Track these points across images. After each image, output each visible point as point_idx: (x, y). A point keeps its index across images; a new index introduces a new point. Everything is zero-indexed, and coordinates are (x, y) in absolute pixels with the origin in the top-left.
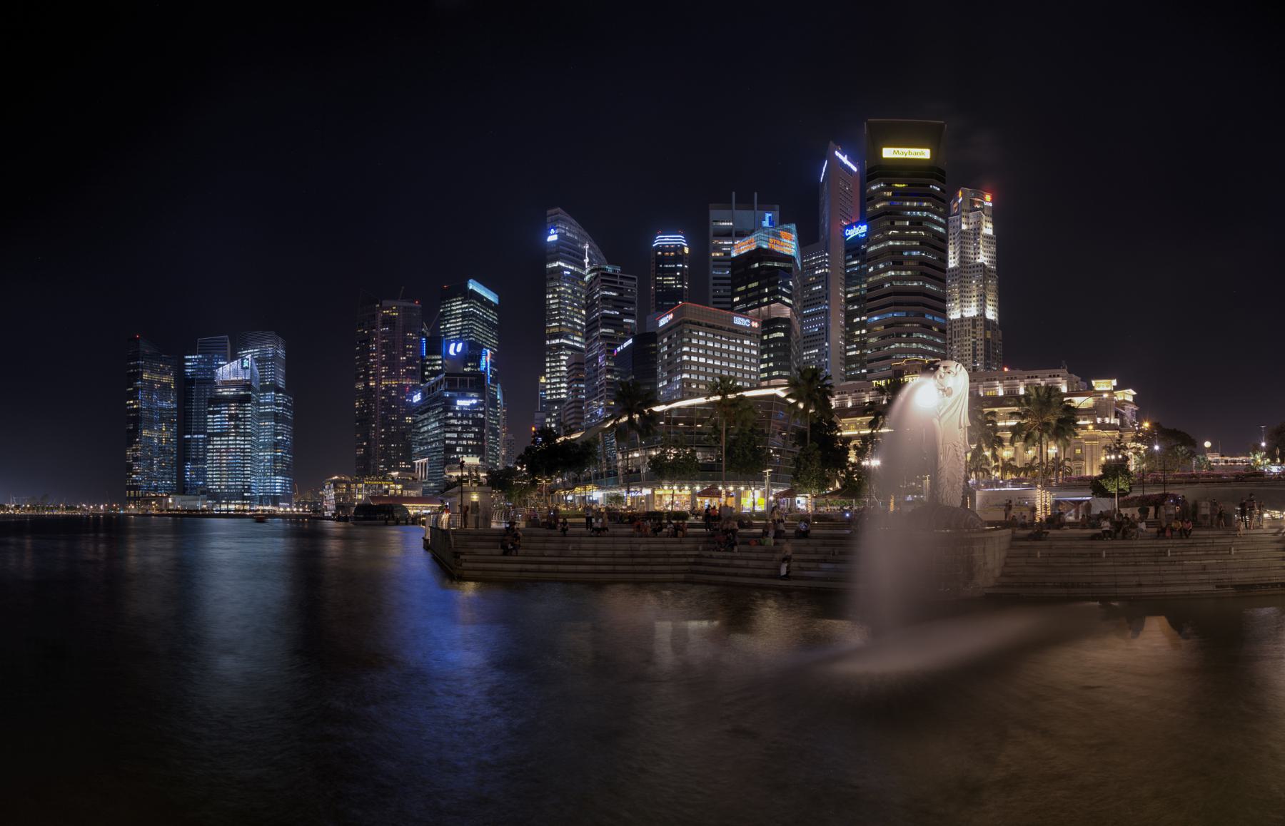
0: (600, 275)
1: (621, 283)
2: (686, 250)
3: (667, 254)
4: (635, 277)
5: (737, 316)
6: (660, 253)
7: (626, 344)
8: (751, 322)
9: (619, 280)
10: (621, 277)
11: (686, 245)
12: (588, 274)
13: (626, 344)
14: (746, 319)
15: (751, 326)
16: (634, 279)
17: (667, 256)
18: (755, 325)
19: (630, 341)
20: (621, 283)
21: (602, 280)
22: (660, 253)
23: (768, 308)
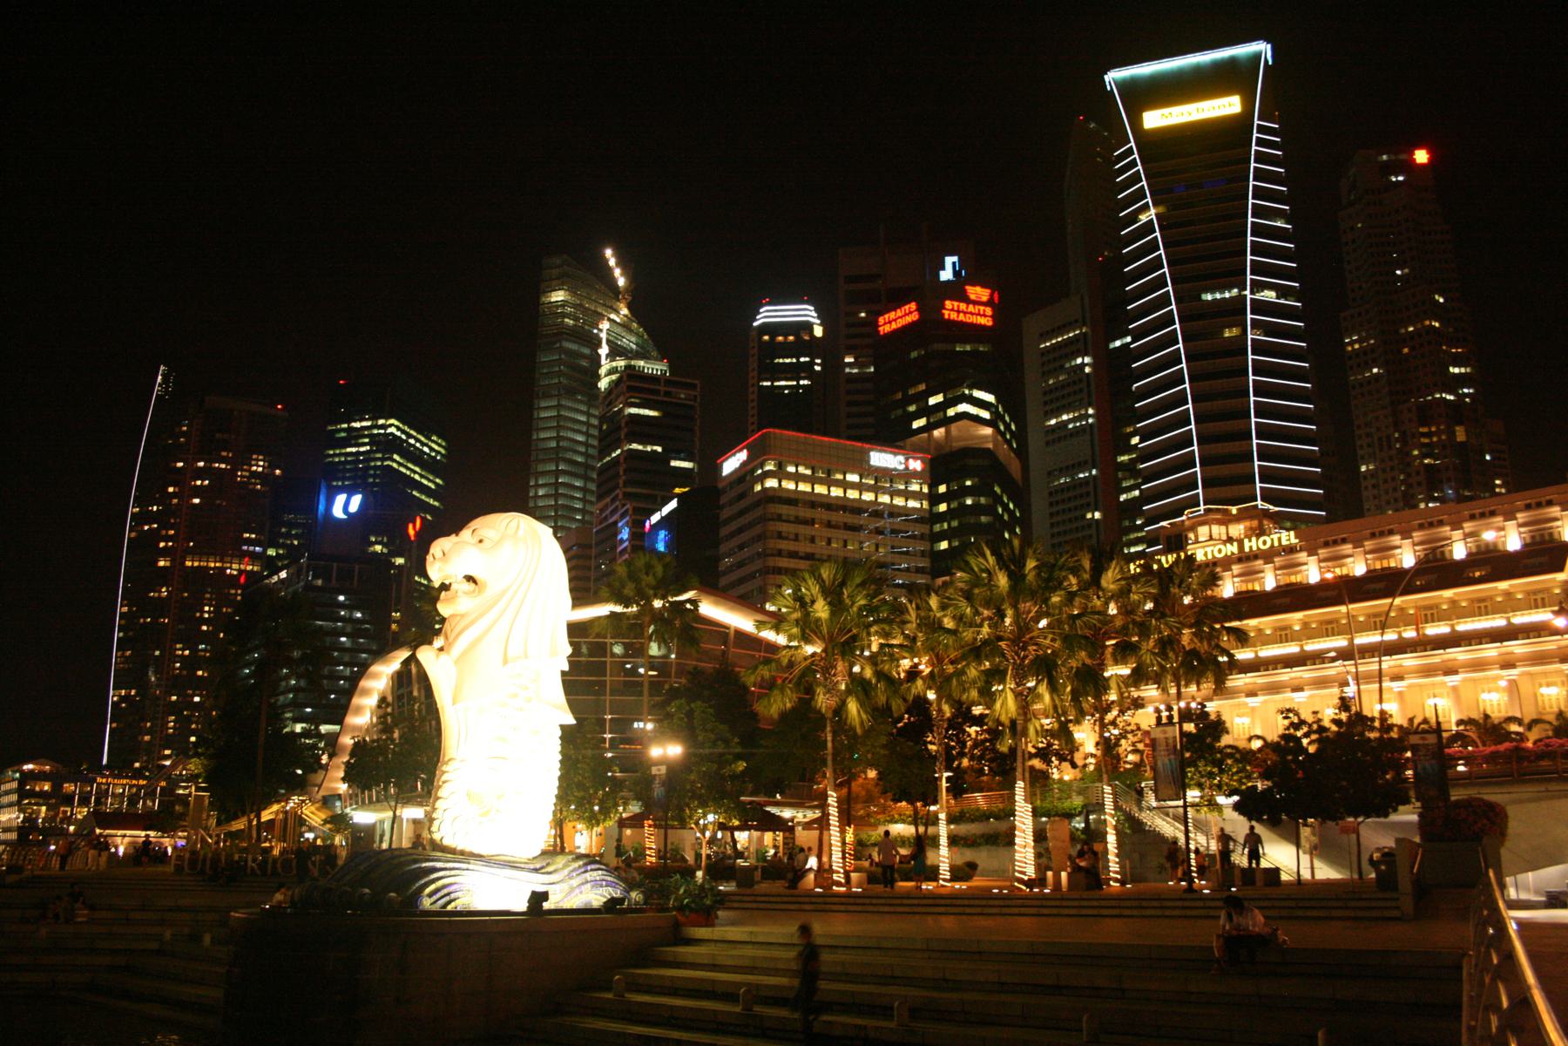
0: (625, 378)
1: (667, 394)
2: (818, 331)
3: (780, 338)
4: (696, 382)
6: (766, 338)
9: (662, 388)
11: (818, 322)
12: (606, 376)
14: (895, 454)
15: (907, 468)
16: (693, 387)
17: (780, 343)
18: (916, 465)
20: (667, 394)
21: (630, 388)
22: (766, 338)
23: (929, 436)
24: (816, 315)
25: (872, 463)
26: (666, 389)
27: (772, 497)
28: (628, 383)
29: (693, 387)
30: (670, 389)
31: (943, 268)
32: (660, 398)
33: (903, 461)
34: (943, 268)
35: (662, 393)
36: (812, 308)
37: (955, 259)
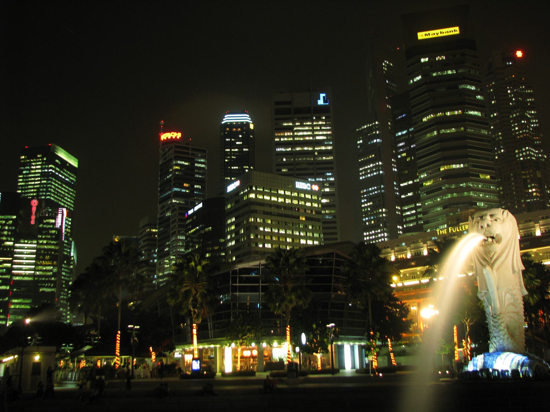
2: (252, 127)
5: (298, 181)
7: (196, 208)
8: (311, 186)
9: (190, 152)
10: (193, 149)
11: (251, 122)
13: (196, 208)
15: (312, 189)
16: (205, 151)
17: (234, 132)
19: (200, 205)
21: (176, 152)
24: (250, 119)
25: (297, 187)
26: (192, 152)
27: (251, 202)
28: (175, 149)
29: (205, 151)
30: (193, 152)
31: (319, 99)
32: (190, 157)
33: (310, 186)
34: (319, 99)
35: (190, 154)
36: (248, 116)
37: (324, 95)
